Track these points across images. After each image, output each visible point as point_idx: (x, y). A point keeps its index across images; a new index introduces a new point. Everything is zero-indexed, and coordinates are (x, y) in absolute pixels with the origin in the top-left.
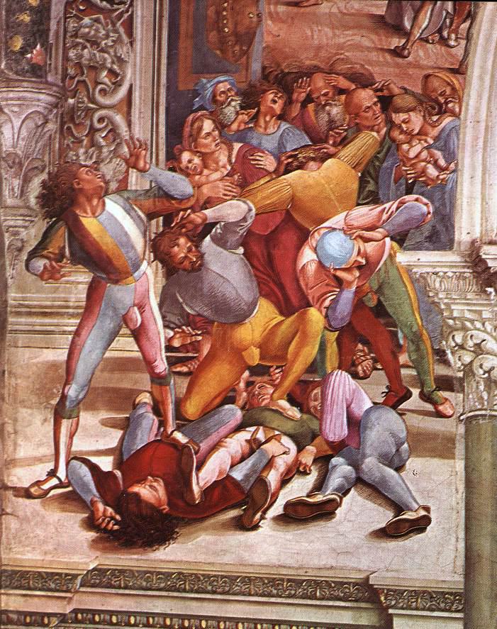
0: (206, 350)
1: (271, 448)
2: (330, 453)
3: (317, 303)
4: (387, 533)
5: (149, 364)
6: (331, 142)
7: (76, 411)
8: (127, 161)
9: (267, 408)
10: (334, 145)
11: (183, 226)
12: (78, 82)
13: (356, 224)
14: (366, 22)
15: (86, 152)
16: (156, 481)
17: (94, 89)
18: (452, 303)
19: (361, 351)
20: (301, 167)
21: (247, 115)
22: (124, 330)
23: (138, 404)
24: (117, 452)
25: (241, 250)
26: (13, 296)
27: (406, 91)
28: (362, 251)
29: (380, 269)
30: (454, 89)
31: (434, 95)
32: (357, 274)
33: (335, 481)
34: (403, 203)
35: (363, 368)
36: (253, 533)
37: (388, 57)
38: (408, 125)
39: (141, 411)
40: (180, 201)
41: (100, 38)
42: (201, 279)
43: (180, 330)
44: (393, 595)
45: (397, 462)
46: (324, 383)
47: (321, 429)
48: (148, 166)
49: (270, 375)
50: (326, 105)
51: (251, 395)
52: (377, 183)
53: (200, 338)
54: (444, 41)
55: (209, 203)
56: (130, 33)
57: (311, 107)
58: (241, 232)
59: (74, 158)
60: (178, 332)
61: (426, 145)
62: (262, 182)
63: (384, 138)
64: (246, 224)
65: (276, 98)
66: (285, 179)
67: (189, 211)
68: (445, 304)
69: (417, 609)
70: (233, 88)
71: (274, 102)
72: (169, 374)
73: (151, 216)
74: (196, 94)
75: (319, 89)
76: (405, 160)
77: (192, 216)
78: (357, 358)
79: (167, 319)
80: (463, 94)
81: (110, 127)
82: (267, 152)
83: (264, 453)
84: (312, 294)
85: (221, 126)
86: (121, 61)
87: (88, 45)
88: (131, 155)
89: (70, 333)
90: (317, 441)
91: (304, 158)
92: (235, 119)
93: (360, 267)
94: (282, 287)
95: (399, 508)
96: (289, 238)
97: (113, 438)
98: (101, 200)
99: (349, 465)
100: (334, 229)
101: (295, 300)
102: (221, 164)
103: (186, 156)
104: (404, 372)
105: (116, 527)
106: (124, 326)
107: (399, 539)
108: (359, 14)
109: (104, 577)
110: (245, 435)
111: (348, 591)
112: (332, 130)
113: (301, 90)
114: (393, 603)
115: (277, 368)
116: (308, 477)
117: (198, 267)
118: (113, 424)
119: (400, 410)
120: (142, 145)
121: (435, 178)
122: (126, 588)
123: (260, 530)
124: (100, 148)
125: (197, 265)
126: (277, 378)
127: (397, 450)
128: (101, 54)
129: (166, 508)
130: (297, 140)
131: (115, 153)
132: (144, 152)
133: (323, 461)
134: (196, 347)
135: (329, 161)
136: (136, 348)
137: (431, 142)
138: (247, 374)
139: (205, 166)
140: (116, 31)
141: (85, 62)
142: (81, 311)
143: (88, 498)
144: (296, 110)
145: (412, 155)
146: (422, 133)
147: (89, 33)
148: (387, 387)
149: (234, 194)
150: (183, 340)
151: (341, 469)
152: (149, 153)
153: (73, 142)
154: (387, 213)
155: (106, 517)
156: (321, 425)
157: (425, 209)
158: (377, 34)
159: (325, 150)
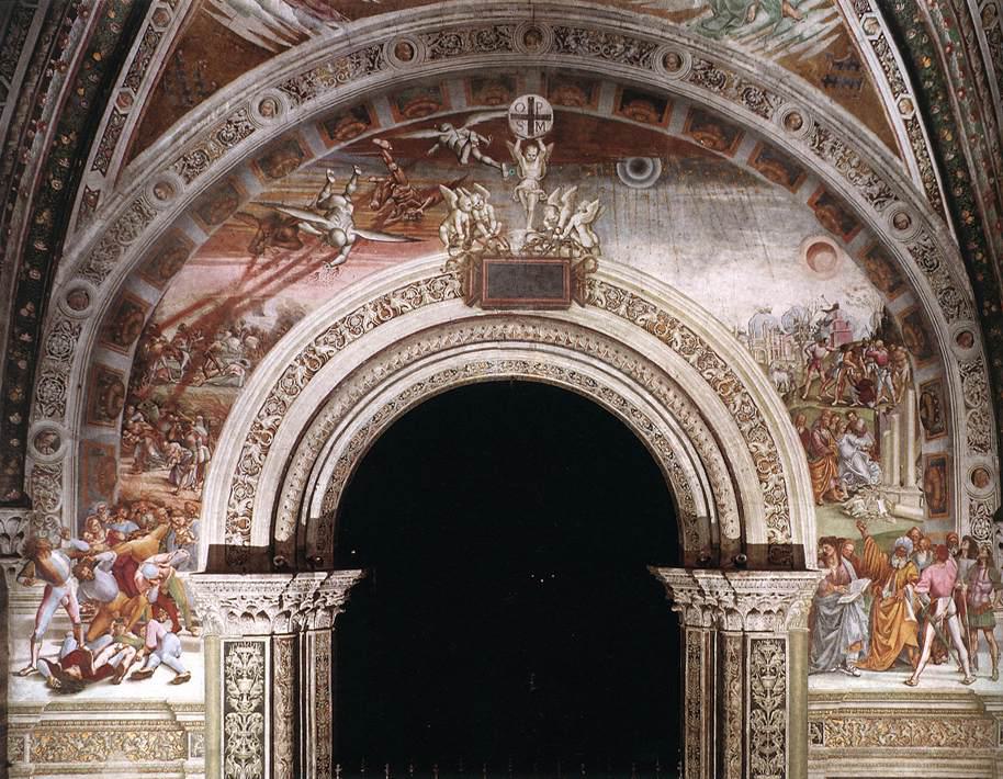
0: (97, 612)
1: (125, 651)
4: (172, 683)
5: (73, 619)
20: (135, 538)
26: (11, 592)
33: (152, 663)
46: (146, 625)
51: (116, 630)
54: (193, 489)
55: (97, 552)
56: (61, 483)
73: (72, 558)
76: (178, 536)
85: (101, 522)
86: (57, 495)
93: (160, 578)
94: (128, 587)
95: (178, 673)
96: (131, 567)
97: (57, 649)
103: (86, 534)
108: (157, 478)
117: (92, 579)
118: (58, 644)
120: (67, 530)
129: (81, 677)
130: (133, 527)
133: (147, 655)
134: (92, 612)
144: (133, 515)
151: (154, 658)
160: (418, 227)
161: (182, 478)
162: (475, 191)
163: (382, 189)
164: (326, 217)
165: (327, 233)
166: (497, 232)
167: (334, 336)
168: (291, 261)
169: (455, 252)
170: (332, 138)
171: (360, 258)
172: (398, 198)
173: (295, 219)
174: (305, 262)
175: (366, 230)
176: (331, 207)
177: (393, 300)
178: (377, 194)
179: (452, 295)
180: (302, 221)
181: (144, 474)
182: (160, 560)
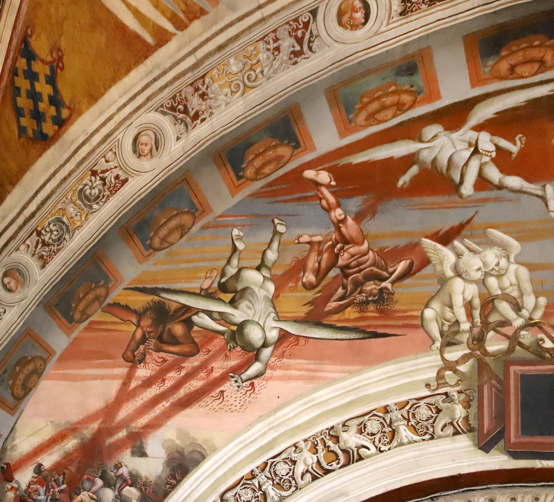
160: (384, 313)
162: (491, 243)
163: (320, 253)
164: (233, 303)
165: (235, 328)
166: (538, 316)
167: (250, 492)
168: (183, 373)
169: (453, 355)
170: (239, 178)
171: (287, 368)
172: (347, 267)
173: (186, 309)
174: (202, 374)
175: (297, 321)
176: (240, 287)
177: (344, 436)
178: (312, 263)
179: (450, 430)
180: (197, 312)
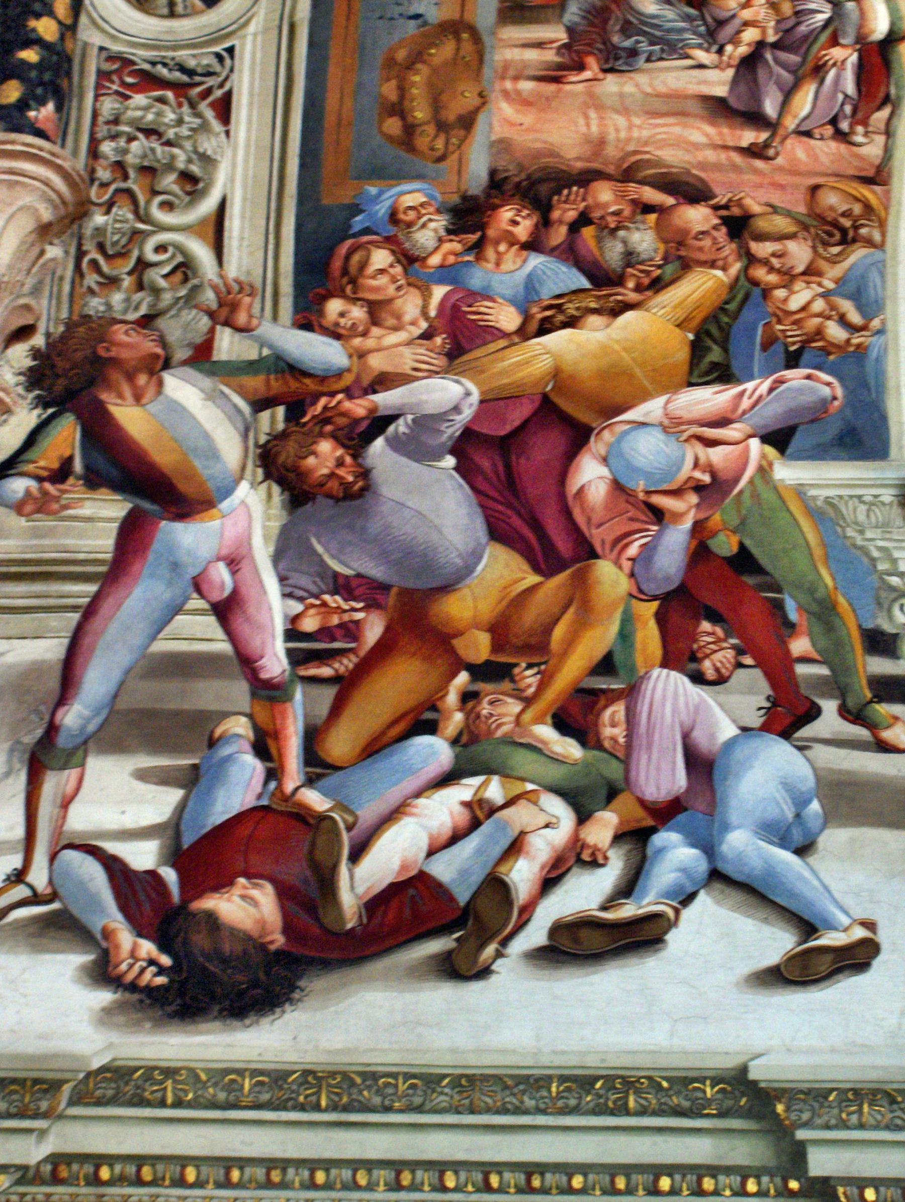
2: (650, 822)
3: (612, 550)
6: (631, 284)
7: (80, 753)
8: (211, 314)
9: (509, 741)
10: (638, 289)
11: (326, 421)
12: (118, 191)
13: (686, 415)
14: (694, 107)
15: (127, 300)
16: (256, 886)
17: (148, 203)
18: (895, 548)
19: (709, 634)
20: (572, 323)
21: (459, 242)
22: (197, 603)
23: (220, 738)
24: (170, 832)
25: (450, 461)
27: (775, 209)
28: (703, 459)
29: (741, 492)
30: (868, 207)
31: (830, 215)
32: (694, 499)
34: (781, 382)
35: (714, 665)
36: (476, 986)
37: (737, 158)
38: (782, 260)
39: (225, 751)
40: (323, 379)
41: (166, 125)
42: (363, 513)
43: (318, 602)
44: (803, 1100)
45: (797, 837)
46: (631, 693)
47: (627, 779)
48: (255, 322)
49: (513, 680)
50: (617, 228)
51: (472, 717)
52: (726, 350)
53: (360, 616)
54: (841, 136)
55: (383, 381)
57: (588, 232)
58: (450, 431)
59: (102, 308)
60: (313, 606)
61: (821, 290)
62: (492, 347)
63: (737, 279)
64: (458, 418)
65: (518, 219)
66: (539, 344)
67: (340, 396)
68: (880, 549)
69: (861, 1126)
70: (433, 202)
71: (515, 223)
72: (292, 681)
74: (356, 209)
75: (606, 205)
76: (782, 315)
77: (347, 405)
78: (700, 648)
79: (290, 582)
80: (887, 213)
81: (179, 259)
82: (500, 301)
83: (504, 826)
84: (598, 536)
86: (207, 160)
87: (141, 136)
88: (221, 305)
89: (74, 608)
90: (620, 801)
91: (578, 309)
92: (436, 249)
93: (699, 488)
94: (536, 525)
98: (155, 378)
99: (693, 845)
100: (643, 424)
101: (563, 545)
102: (407, 318)
103: (334, 306)
104: (801, 669)
105: (161, 980)
106: (195, 595)
107: (812, 988)
109: (127, 1083)
110: (465, 790)
111: (700, 1095)
112: (633, 267)
113: (567, 206)
114: (806, 1116)
115: (530, 666)
116: (601, 872)
118: (163, 778)
119: (798, 739)
121: (842, 343)
122: (179, 1104)
123: (494, 978)
124: (156, 292)
125: (357, 487)
126: (529, 686)
127: (798, 816)
128: (167, 148)
129: (278, 940)
131: (190, 300)
132: (247, 300)
134: (352, 631)
135: (629, 315)
136: (219, 633)
137: (831, 285)
138: (463, 677)
139: (375, 320)
140: (199, 115)
141: (130, 159)
142: (103, 569)
143: (96, 924)
144: (559, 235)
145: (795, 303)
146: (811, 272)
147: (142, 118)
148: (768, 698)
149: (432, 368)
150: (324, 618)
152: (258, 300)
153: (99, 283)
154: (750, 398)
155: (137, 960)
156: (627, 771)
157: (827, 391)
158: (713, 124)
159: (619, 298)
161: (788, 94)
181: (611, 84)
182: (698, 412)
